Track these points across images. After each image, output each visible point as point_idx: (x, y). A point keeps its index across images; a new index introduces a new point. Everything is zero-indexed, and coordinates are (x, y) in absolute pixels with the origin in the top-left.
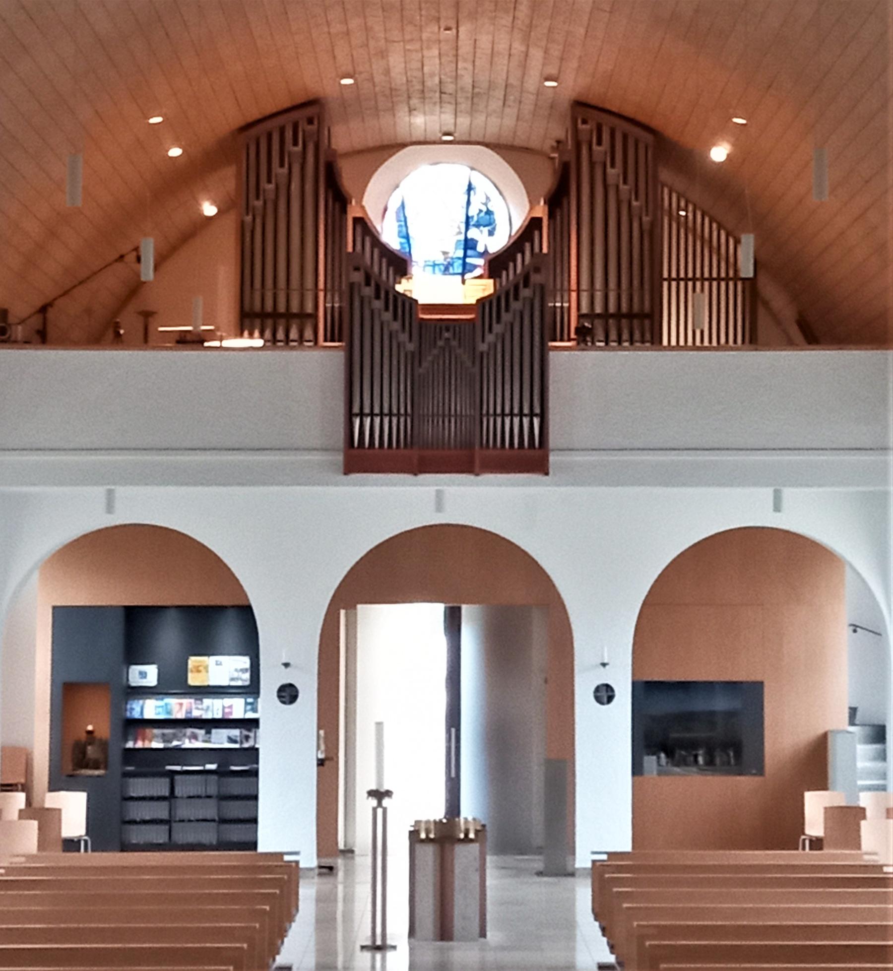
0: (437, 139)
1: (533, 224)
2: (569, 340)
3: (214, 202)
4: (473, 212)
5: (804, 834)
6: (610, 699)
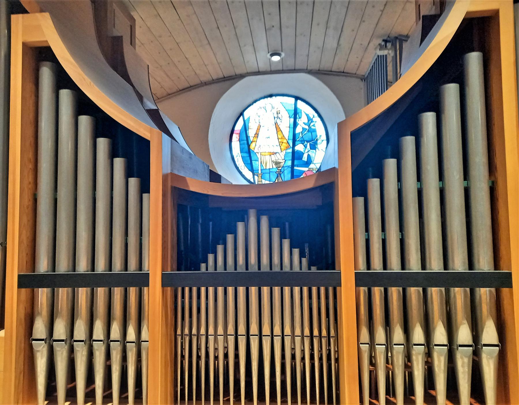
4: (299, 130)
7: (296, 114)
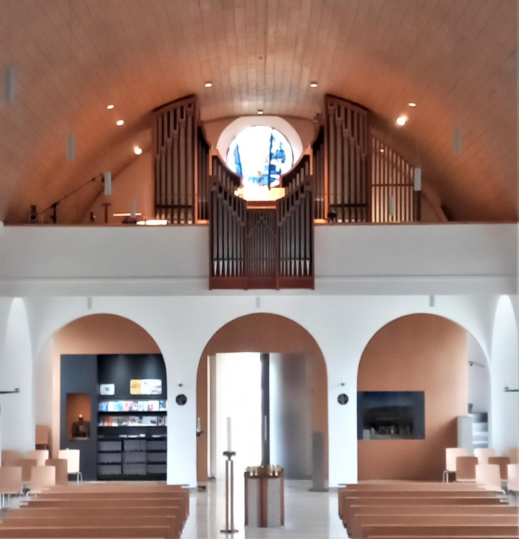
0: (255, 113)
1: (305, 159)
2: (324, 218)
3: (140, 147)
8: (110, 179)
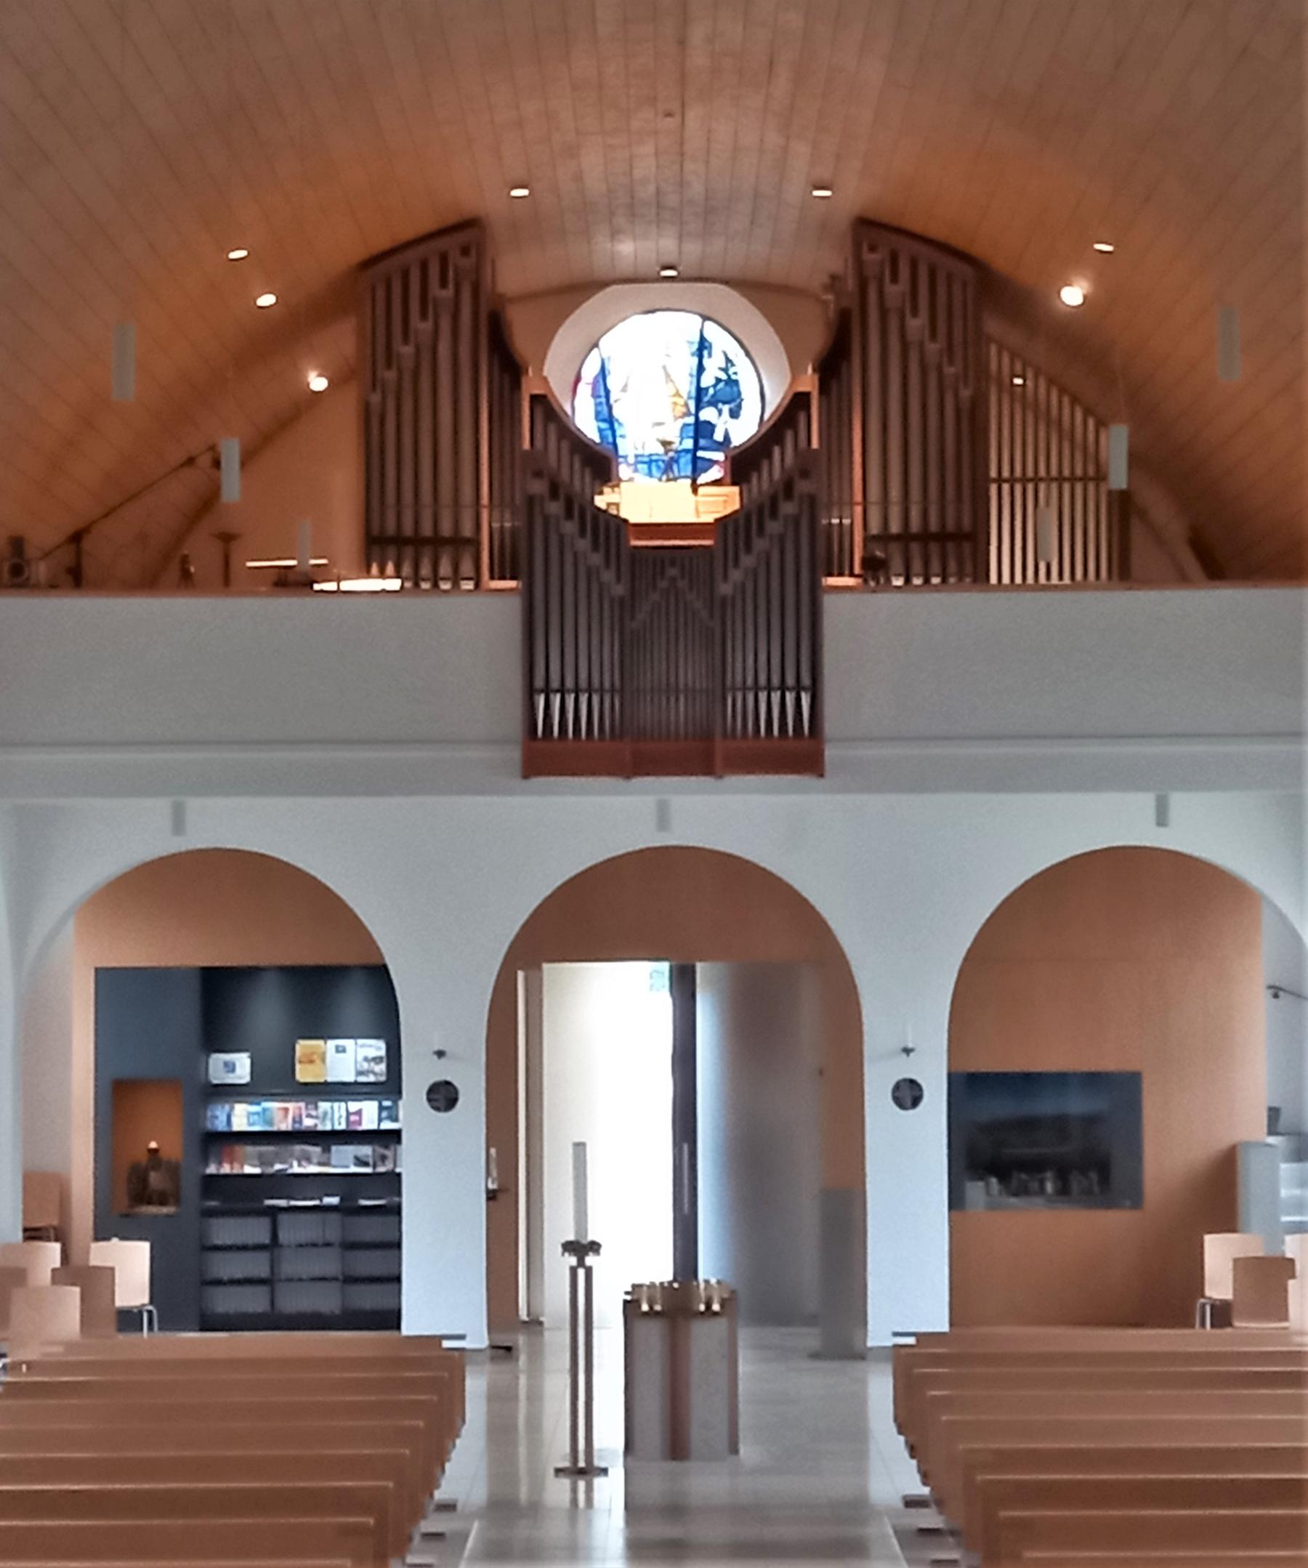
1: (798, 403)
2: (852, 575)
4: (707, 381)
5: (1203, 1296)
6: (916, 1101)
7: (703, 346)
8: (236, 465)
